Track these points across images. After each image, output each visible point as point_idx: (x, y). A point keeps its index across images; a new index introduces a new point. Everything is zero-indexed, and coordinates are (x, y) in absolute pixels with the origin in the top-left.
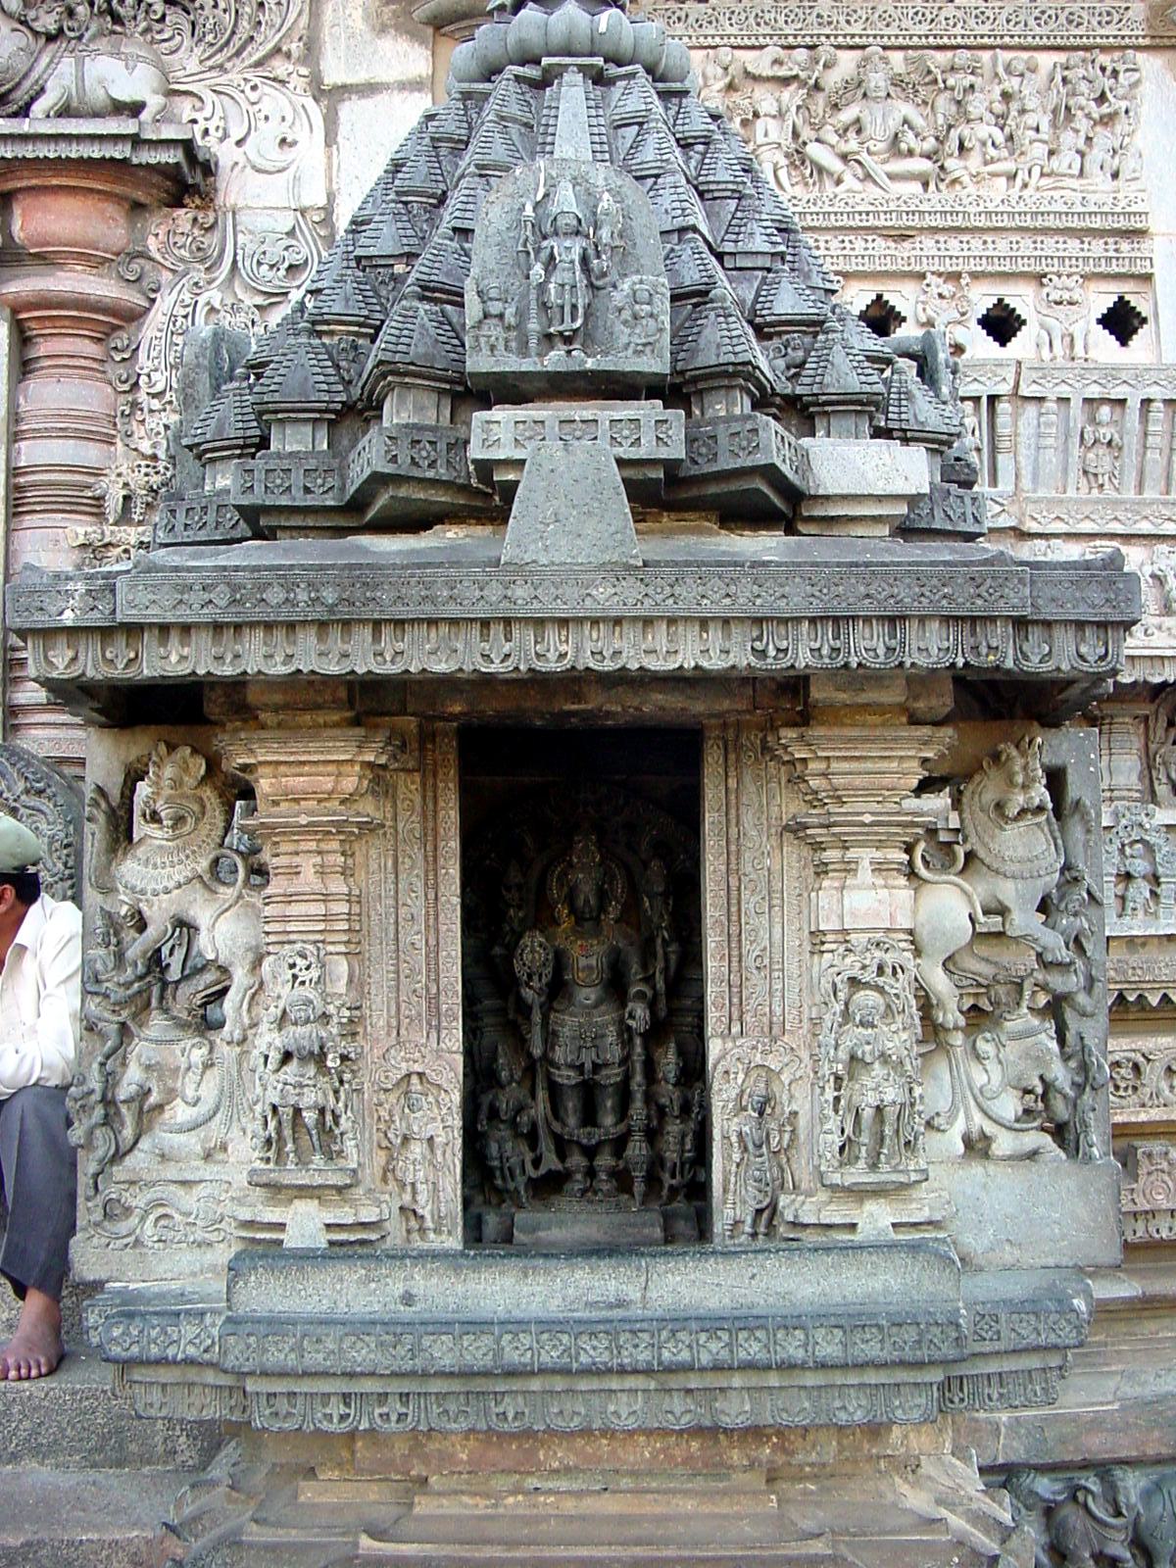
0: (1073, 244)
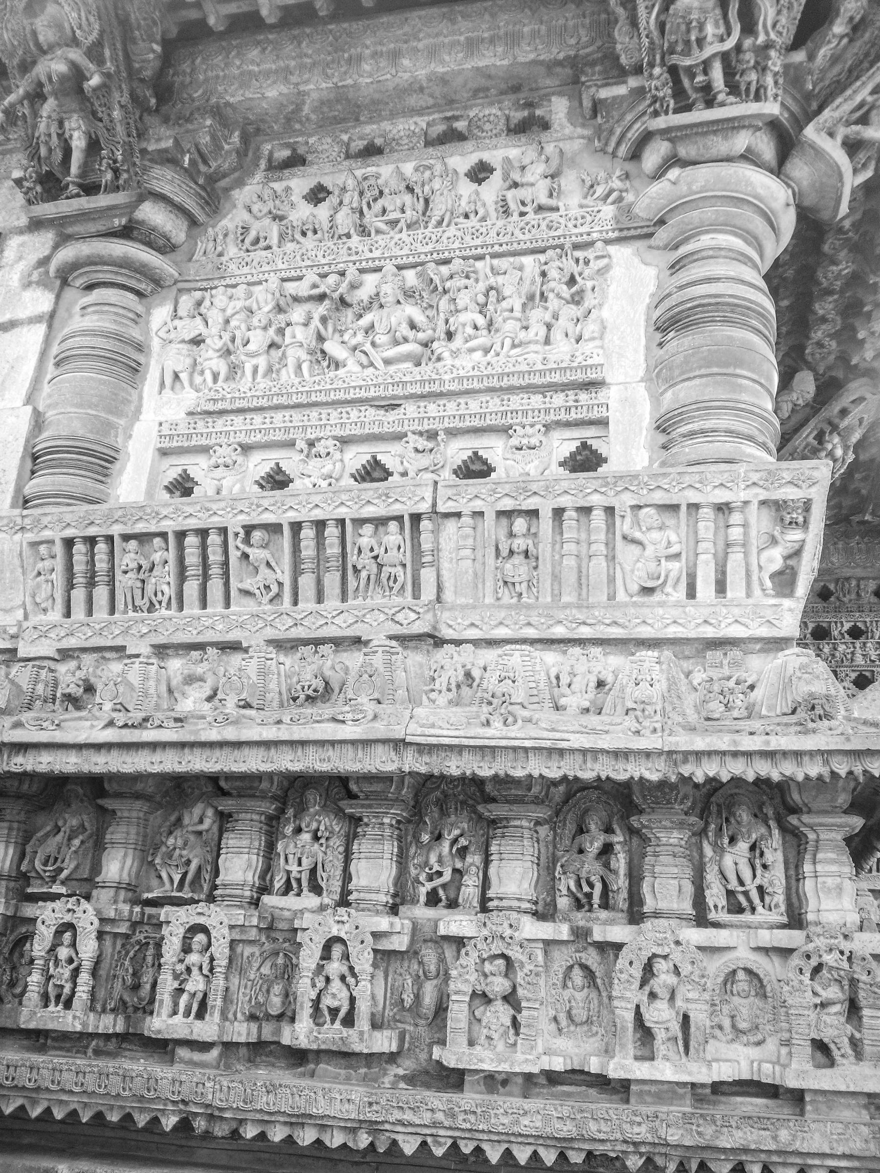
0: (536, 400)
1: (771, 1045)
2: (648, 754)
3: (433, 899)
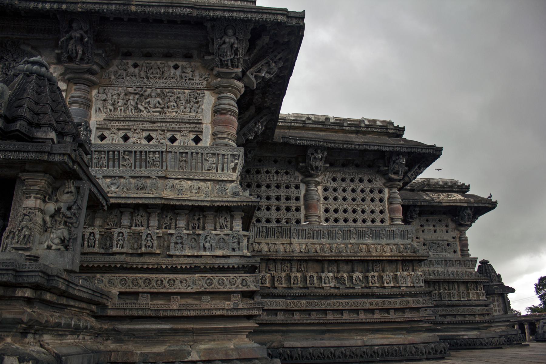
0: (187, 125)
1: (226, 250)
2: (207, 201)
3: (166, 228)
